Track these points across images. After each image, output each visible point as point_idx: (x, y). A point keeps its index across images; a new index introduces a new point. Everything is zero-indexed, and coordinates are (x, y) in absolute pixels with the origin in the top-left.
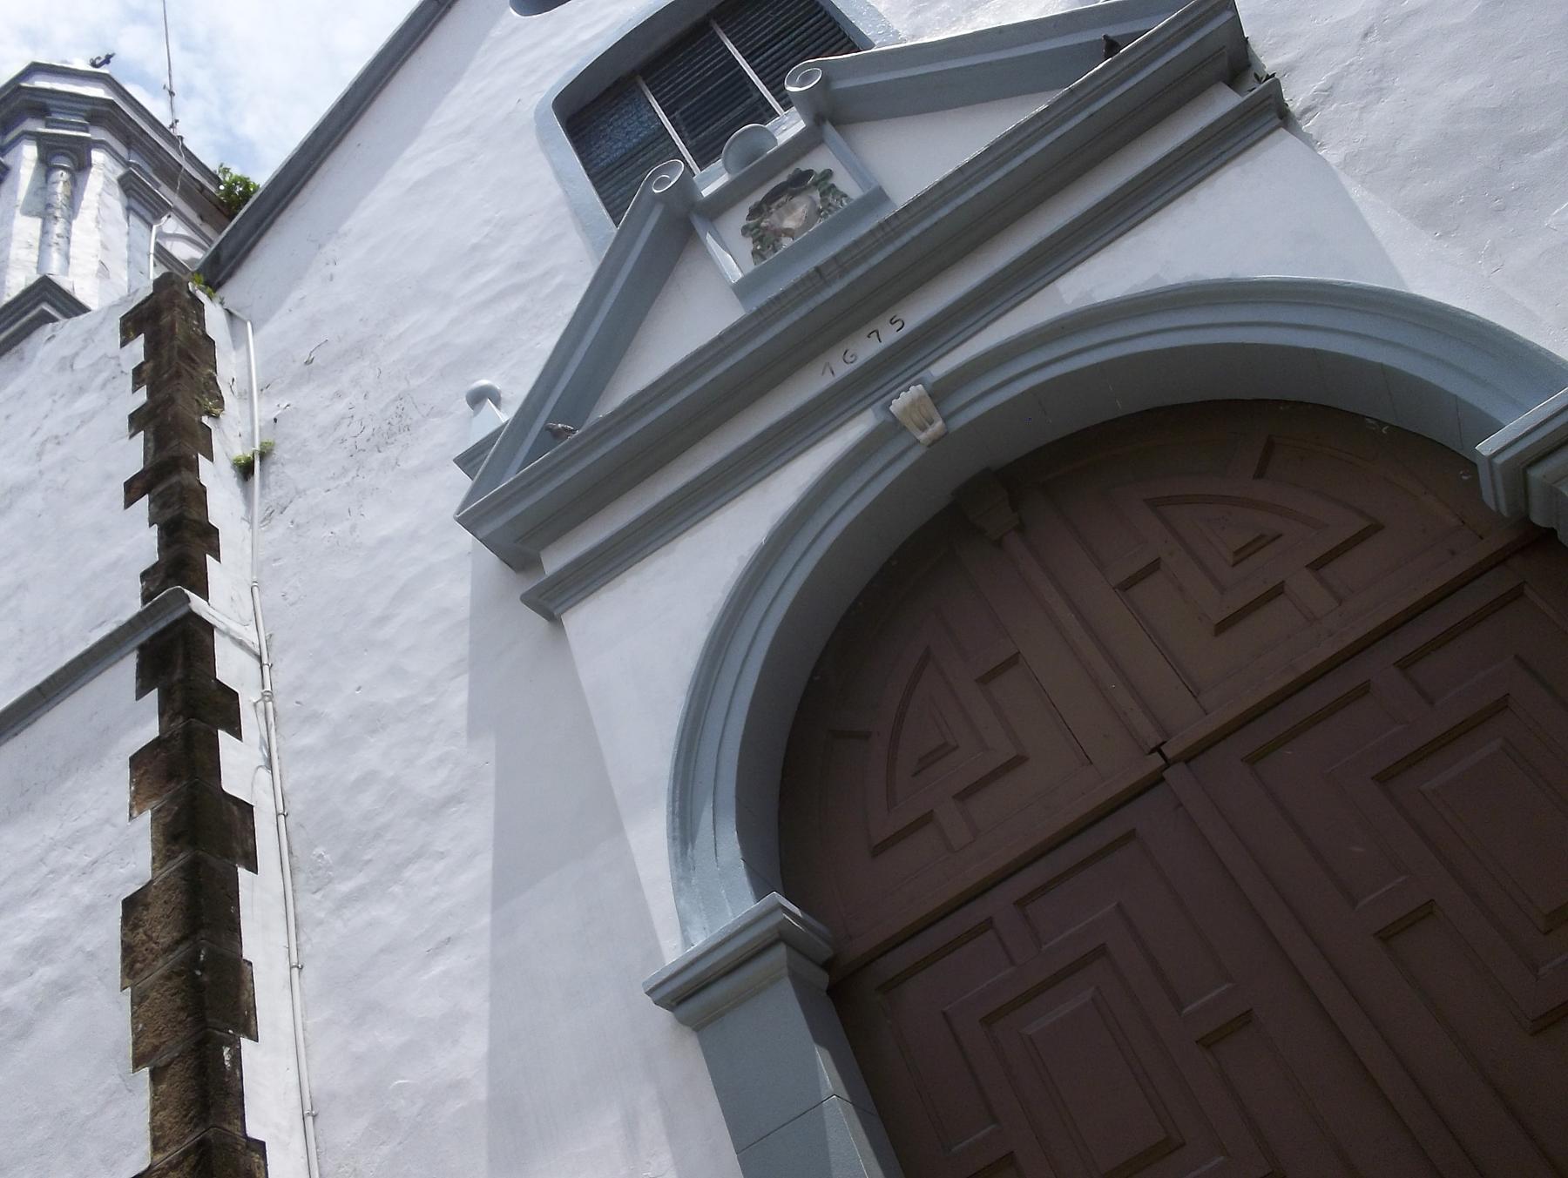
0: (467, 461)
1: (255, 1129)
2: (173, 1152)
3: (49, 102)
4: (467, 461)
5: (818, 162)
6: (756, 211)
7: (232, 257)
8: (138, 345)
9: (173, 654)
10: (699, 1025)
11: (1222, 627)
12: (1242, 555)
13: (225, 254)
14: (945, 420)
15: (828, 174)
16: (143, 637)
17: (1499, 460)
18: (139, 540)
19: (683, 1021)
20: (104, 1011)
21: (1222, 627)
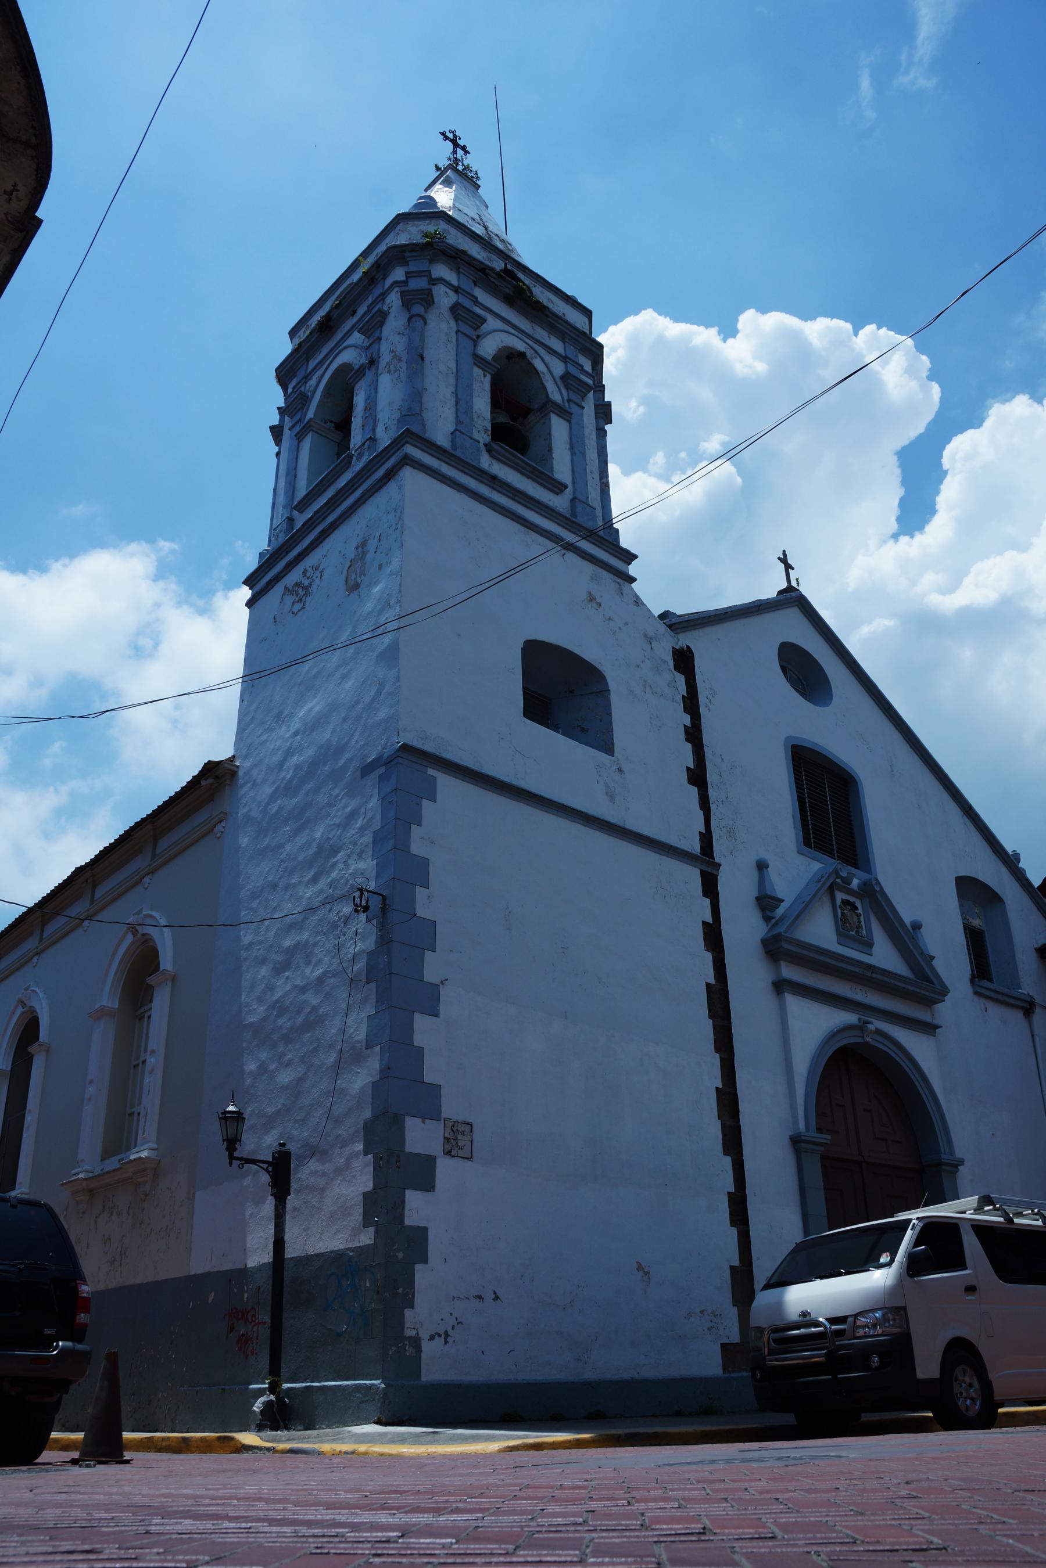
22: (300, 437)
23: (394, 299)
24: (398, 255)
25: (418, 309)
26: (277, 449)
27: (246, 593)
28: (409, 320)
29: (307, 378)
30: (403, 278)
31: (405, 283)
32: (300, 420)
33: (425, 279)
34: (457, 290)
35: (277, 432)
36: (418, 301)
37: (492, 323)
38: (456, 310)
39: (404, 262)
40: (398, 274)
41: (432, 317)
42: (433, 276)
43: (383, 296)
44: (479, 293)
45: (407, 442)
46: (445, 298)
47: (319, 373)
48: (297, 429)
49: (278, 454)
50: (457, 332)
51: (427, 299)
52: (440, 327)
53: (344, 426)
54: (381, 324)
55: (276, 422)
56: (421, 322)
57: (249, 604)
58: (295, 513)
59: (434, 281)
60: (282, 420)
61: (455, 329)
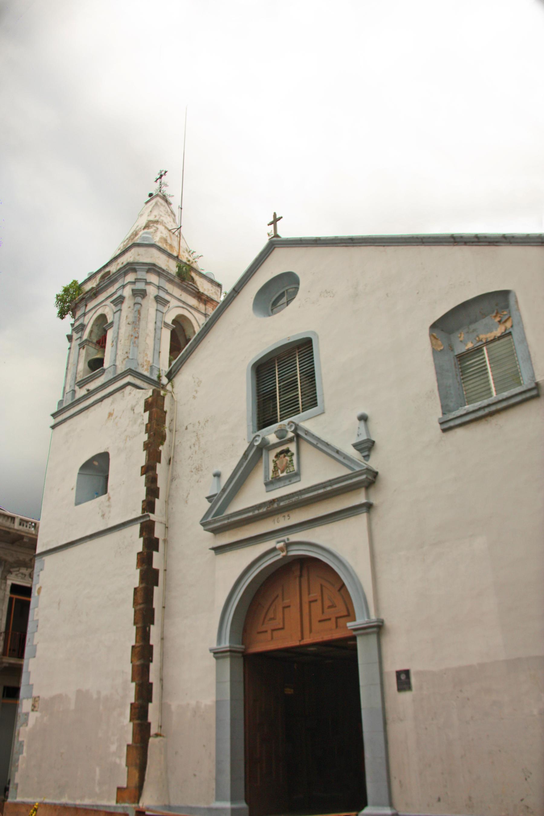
0: (209, 498)
1: (151, 642)
2: (138, 645)
3: (137, 267)
4: (209, 498)
5: (292, 447)
6: (277, 456)
7: (174, 371)
8: (147, 413)
9: (147, 529)
10: (217, 658)
11: (320, 621)
12: (329, 607)
13: (173, 371)
14: (287, 552)
15: (293, 454)
16: (142, 521)
17: (349, 628)
18: (142, 493)
19: (215, 657)
20: (128, 612)
21: (320, 621)
22: (82, 346)
23: (127, 292)
24: (131, 267)
25: (139, 299)
26: (68, 345)
27: (52, 422)
28: (135, 304)
29: (85, 314)
30: (133, 280)
31: (134, 283)
32: (81, 338)
33: (144, 284)
34: (159, 288)
35: (70, 338)
36: (141, 294)
37: (173, 303)
38: (158, 299)
39: (134, 270)
40: (130, 277)
41: (144, 302)
42: (148, 281)
43: (124, 286)
44: (168, 287)
45: (130, 374)
46: (152, 291)
47: (90, 315)
48: (79, 342)
49: (70, 348)
50: (157, 310)
51: (143, 294)
52: (150, 307)
53: (101, 343)
54: (122, 302)
55: (70, 333)
56: (140, 306)
57: (53, 427)
58: (77, 388)
59: (148, 283)
60: (72, 332)
61: (155, 308)
